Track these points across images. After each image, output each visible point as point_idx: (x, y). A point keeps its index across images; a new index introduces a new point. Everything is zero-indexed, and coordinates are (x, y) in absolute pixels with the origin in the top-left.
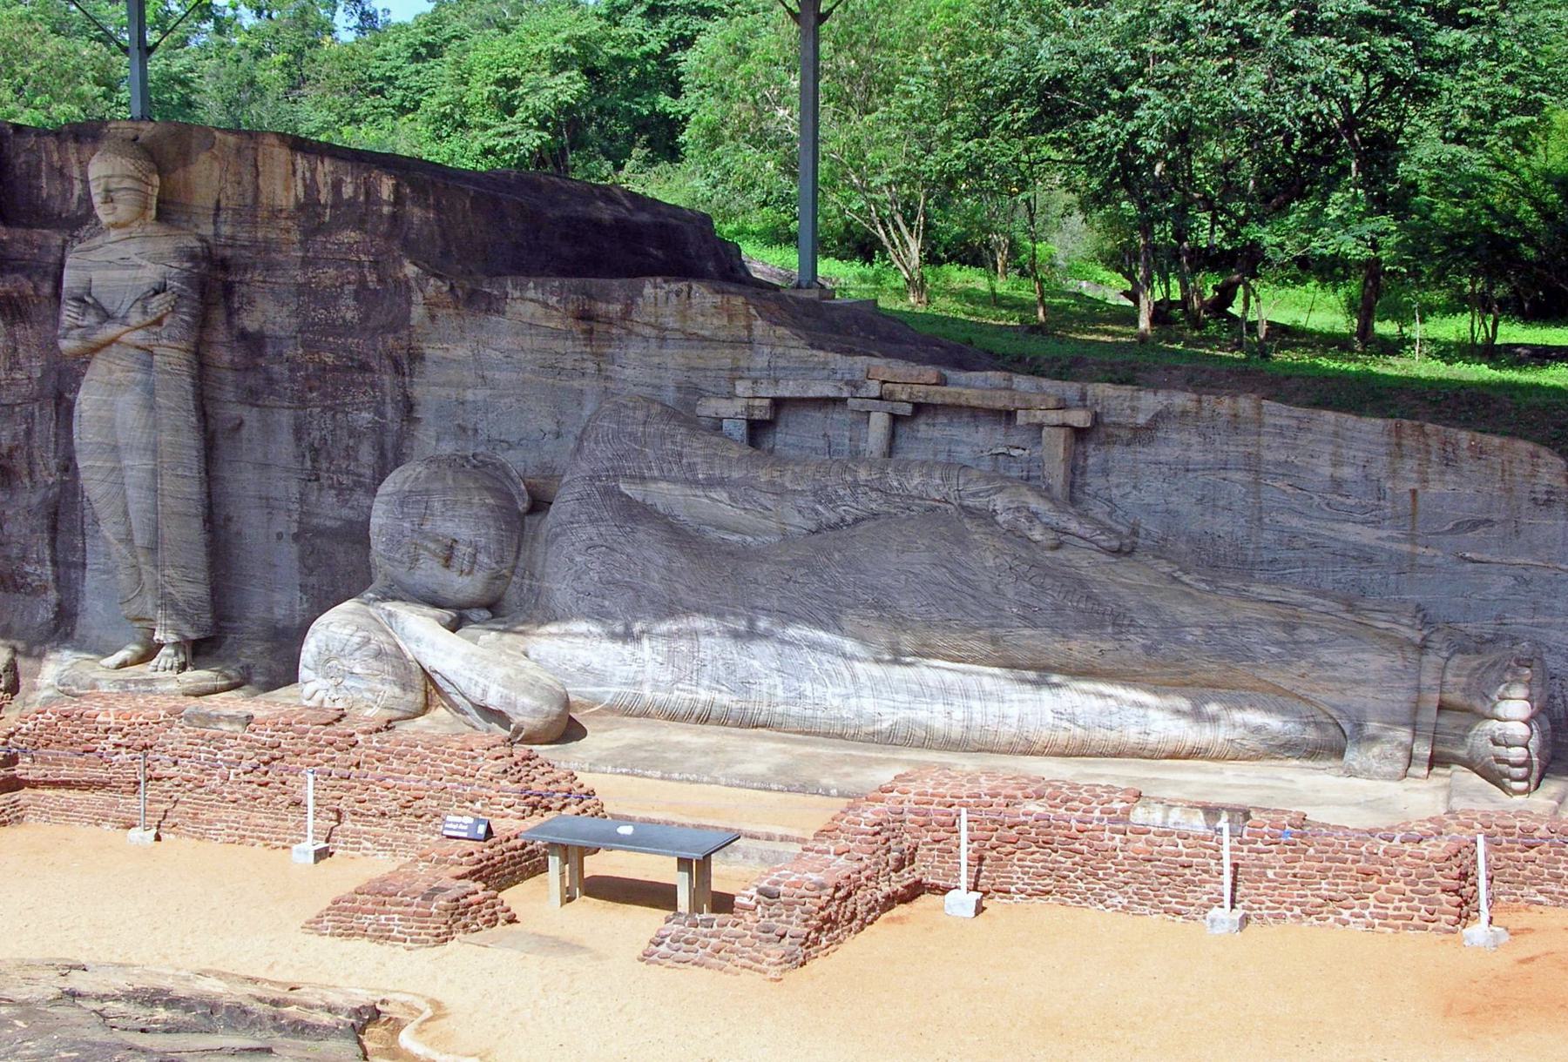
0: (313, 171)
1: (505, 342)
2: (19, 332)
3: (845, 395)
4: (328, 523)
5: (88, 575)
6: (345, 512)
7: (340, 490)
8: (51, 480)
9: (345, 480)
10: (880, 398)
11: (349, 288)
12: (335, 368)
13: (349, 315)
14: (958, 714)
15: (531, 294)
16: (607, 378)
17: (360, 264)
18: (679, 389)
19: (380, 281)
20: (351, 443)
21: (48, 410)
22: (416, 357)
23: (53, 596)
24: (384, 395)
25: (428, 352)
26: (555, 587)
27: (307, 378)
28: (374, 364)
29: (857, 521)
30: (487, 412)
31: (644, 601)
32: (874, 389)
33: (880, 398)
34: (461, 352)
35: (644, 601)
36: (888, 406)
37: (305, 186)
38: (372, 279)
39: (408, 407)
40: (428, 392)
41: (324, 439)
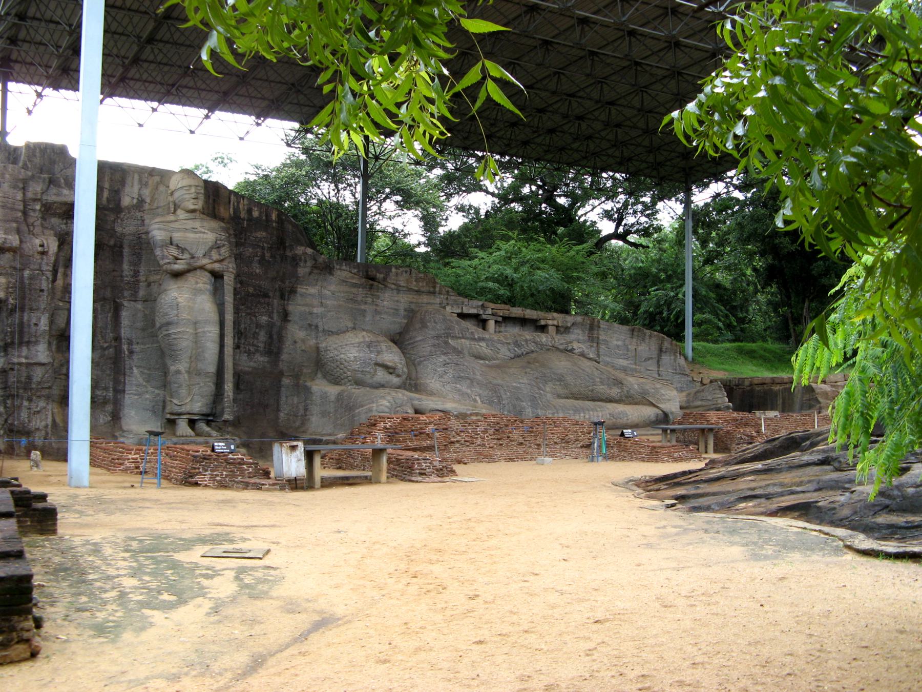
0: (238, 203)
1: (333, 288)
3: (481, 312)
4: (247, 369)
5: (126, 396)
6: (252, 364)
7: (249, 353)
8: (106, 345)
9: (252, 349)
10: (493, 314)
11: (256, 259)
12: (253, 295)
13: (257, 271)
14: (587, 417)
15: (344, 267)
16: (377, 305)
17: (263, 248)
18: (405, 310)
19: (271, 257)
21: (108, 307)
22: (293, 291)
23: (109, 408)
24: (273, 309)
25: (299, 290)
26: (428, 381)
27: (240, 299)
28: (271, 294)
29: (527, 353)
31: (475, 384)
32: (489, 311)
33: (493, 314)
35: (475, 384)
36: (495, 318)
37: (234, 209)
38: (267, 255)
39: (285, 316)
40: (296, 308)
41: (246, 328)
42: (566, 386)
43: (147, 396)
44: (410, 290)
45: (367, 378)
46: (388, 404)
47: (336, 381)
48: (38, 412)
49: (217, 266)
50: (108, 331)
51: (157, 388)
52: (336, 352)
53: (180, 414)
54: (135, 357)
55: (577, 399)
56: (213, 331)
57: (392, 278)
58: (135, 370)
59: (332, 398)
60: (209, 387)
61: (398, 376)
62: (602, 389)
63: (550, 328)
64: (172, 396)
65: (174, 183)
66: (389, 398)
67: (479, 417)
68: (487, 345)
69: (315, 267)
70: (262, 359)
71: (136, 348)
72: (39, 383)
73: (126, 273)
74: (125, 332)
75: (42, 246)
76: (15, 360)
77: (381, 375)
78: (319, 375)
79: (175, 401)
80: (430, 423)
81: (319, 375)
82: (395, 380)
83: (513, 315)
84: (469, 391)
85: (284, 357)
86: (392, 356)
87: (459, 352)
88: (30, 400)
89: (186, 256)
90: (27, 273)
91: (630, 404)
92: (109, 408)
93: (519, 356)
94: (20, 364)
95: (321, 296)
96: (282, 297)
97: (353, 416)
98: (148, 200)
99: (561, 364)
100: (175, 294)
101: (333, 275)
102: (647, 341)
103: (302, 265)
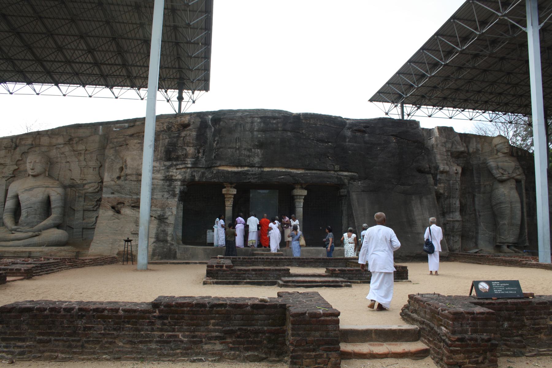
48: (456, 242)
49: (519, 177)
56: (518, 205)
60: (517, 231)
65: (495, 142)
71: (481, 214)
72: (457, 229)
73: (476, 181)
74: (477, 207)
76: (448, 219)
88: (453, 237)
89: (506, 173)
90: (451, 182)
92: (474, 240)
94: (450, 221)
98: (480, 149)
100: (503, 190)
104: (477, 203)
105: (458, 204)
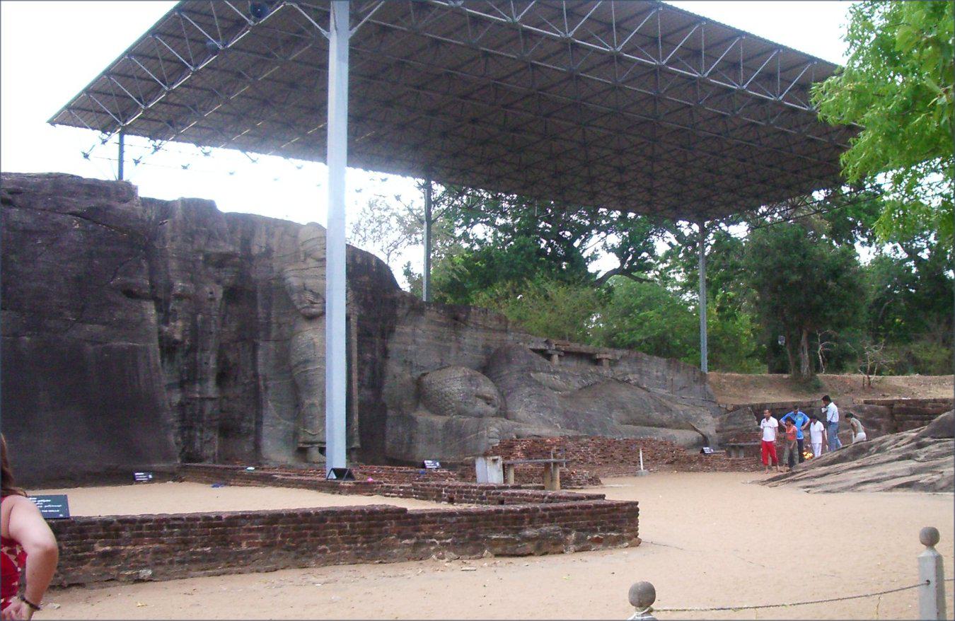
2: (229, 307)
5: (264, 428)
10: (557, 349)
18: (483, 347)
20: (363, 367)
22: (392, 331)
23: (251, 438)
25: (397, 329)
28: (373, 333)
30: (415, 355)
32: (554, 347)
33: (557, 349)
34: (408, 330)
36: (558, 353)
39: (385, 353)
40: (394, 346)
42: (628, 413)
43: (281, 428)
44: (486, 329)
45: (470, 410)
46: (497, 431)
47: (440, 412)
50: (249, 368)
51: (288, 420)
52: (440, 386)
53: (312, 443)
54: (270, 392)
55: (635, 424)
57: (472, 319)
58: (270, 404)
59: (440, 427)
61: (494, 406)
62: (656, 415)
63: (604, 360)
64: (305, 427)
66: (497, 425)
67: (588, 439)
68: (561, 378)
69: (412, 309)
70: (366, 393)
71: (271, 384)
72: (210, 416)
74: (261, 370)
75: (211, 293)
77: (481, 406)
78: (421, 406)
79: (309, 431)
80: (553, 445)
81: (421, 406)
82: (491, 410)
83: (573, 350)
84: (551, 419)
85: (385, 390)
86: (488, 389)
87: (540, 384)
88: (202, 431)
91: (677, 428)
92: (251, 438)
93: (585, 387)
95: (414, 334)
96: (383, 336)
97: (465, 442)
99: (624, 394)
100: (311, 335)
101: (423, 315)
102: (681, 371)
103: (400, 306)
104: (260, 360)
105: (212, 364)
